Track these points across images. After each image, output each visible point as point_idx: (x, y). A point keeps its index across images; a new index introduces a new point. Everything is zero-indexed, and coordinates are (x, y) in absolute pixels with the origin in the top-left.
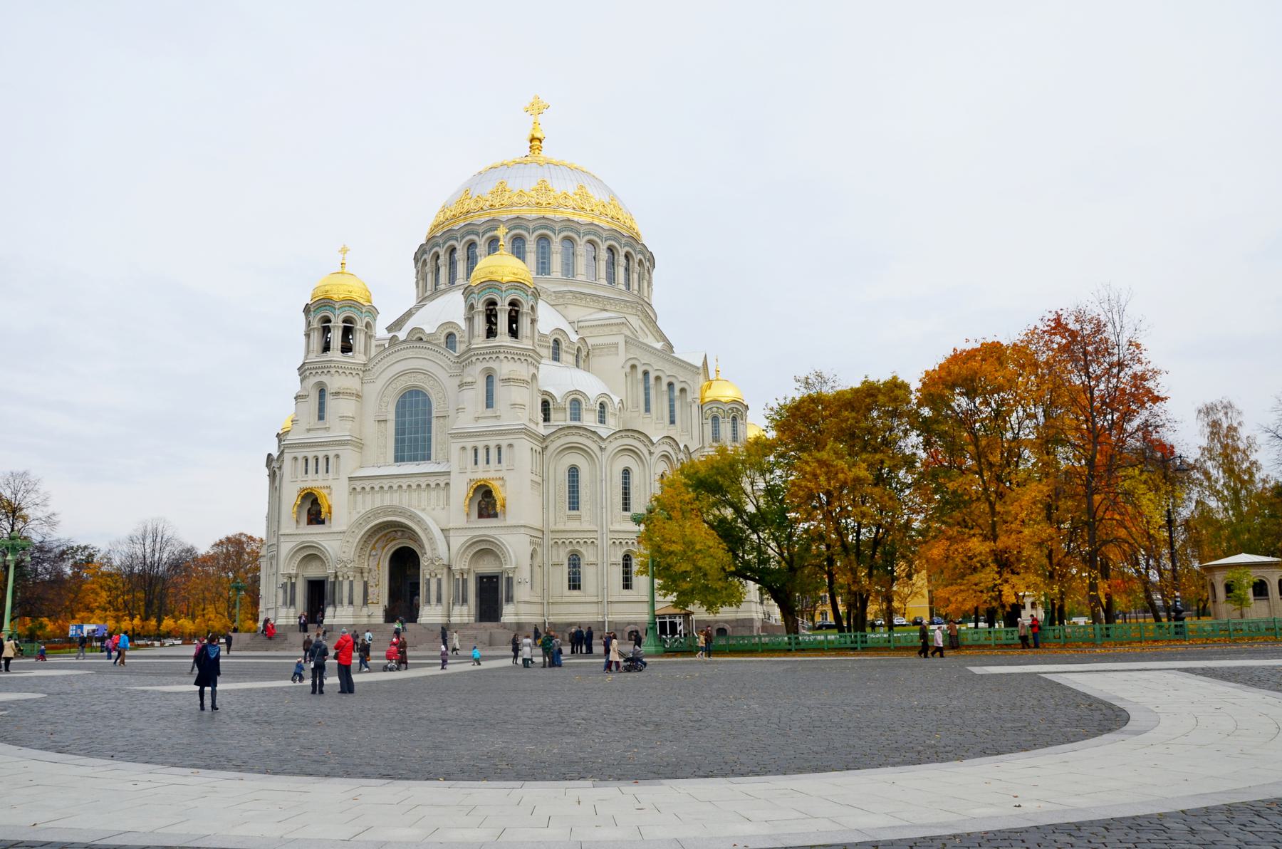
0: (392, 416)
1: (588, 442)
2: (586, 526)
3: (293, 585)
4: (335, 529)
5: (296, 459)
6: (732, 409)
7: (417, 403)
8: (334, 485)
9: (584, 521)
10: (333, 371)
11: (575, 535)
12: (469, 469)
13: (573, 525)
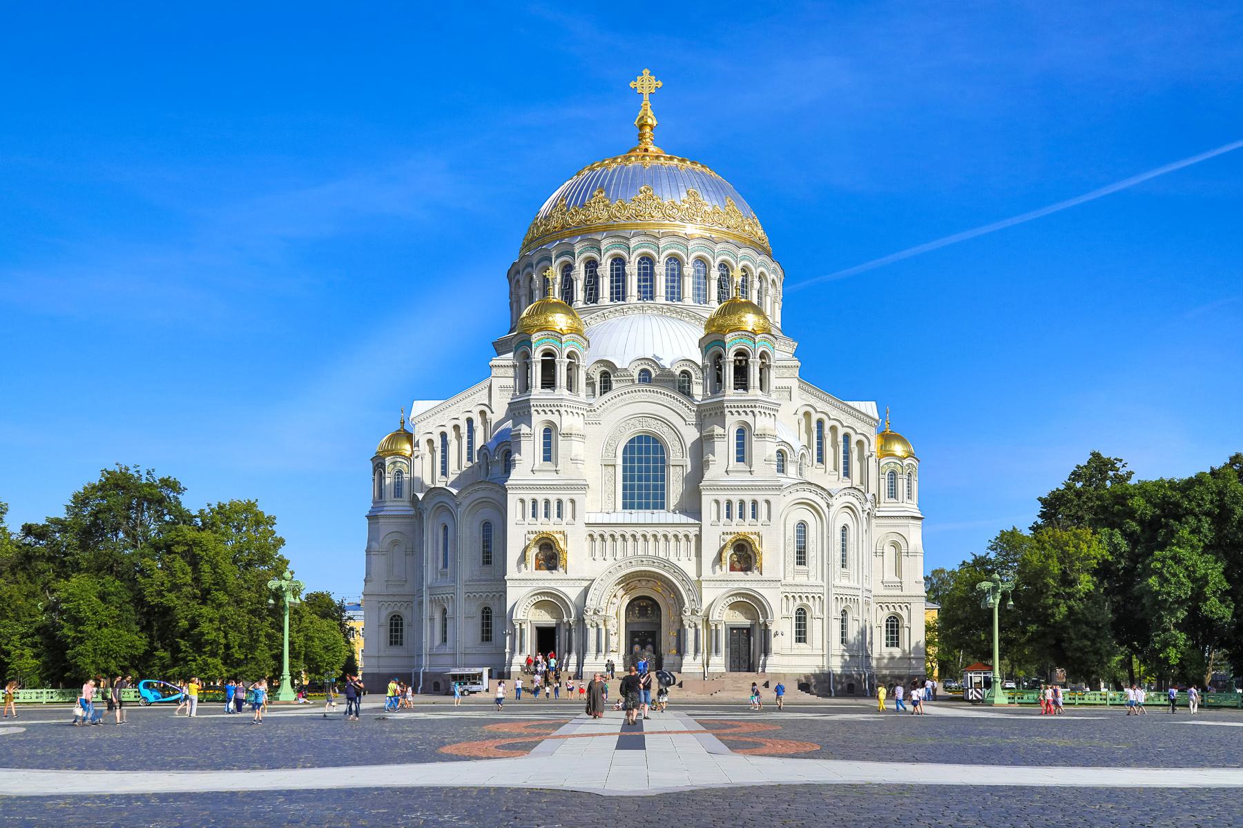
0: (620, 461)
1: (818, 499)
2: (812, 581)
3: (522, 630)
4: (570, 575)
5: (522, 501)
6: (908, 465)
7: (648, 448)
8: (568, 530)
9: (810, 577)
10: (562, 410)
11: (804, 590)
12: (721, 523)
13: (801, 579)
